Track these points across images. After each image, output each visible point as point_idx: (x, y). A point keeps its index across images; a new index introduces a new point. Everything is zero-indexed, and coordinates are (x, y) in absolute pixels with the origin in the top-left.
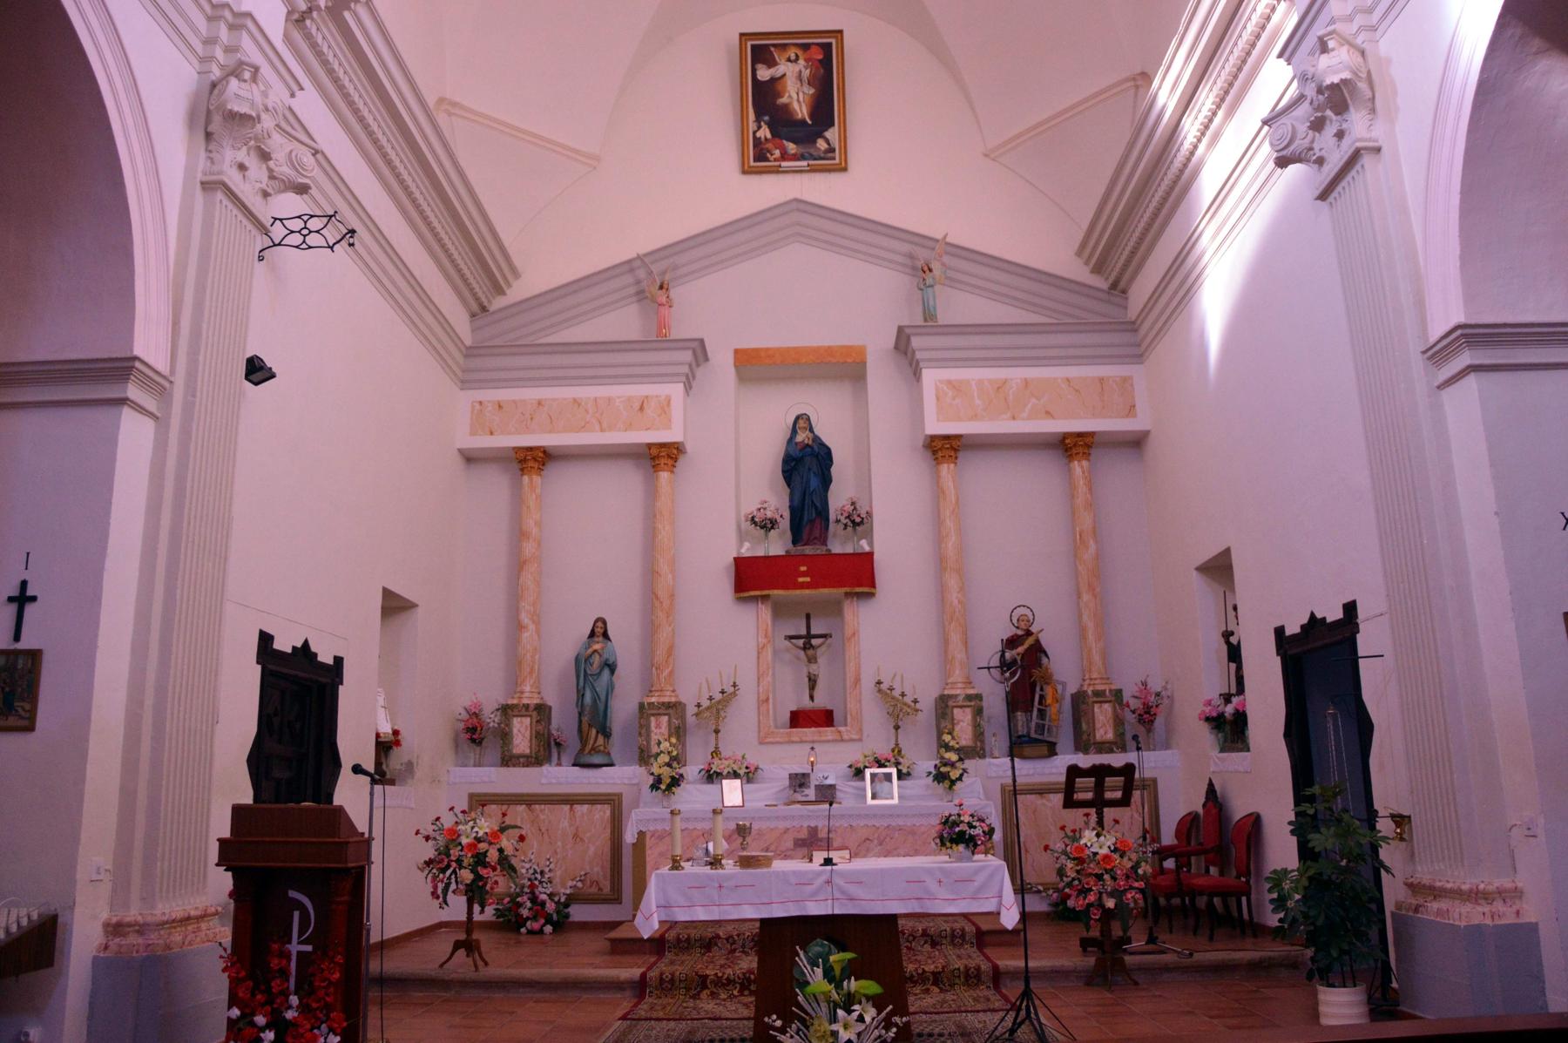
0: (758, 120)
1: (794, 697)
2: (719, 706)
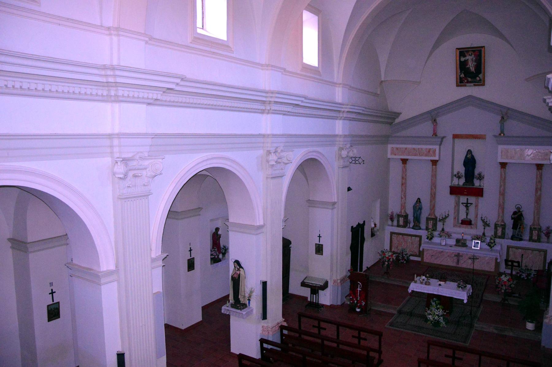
0: (461, 72)
1: (463, 216)
2: (443, 220)
